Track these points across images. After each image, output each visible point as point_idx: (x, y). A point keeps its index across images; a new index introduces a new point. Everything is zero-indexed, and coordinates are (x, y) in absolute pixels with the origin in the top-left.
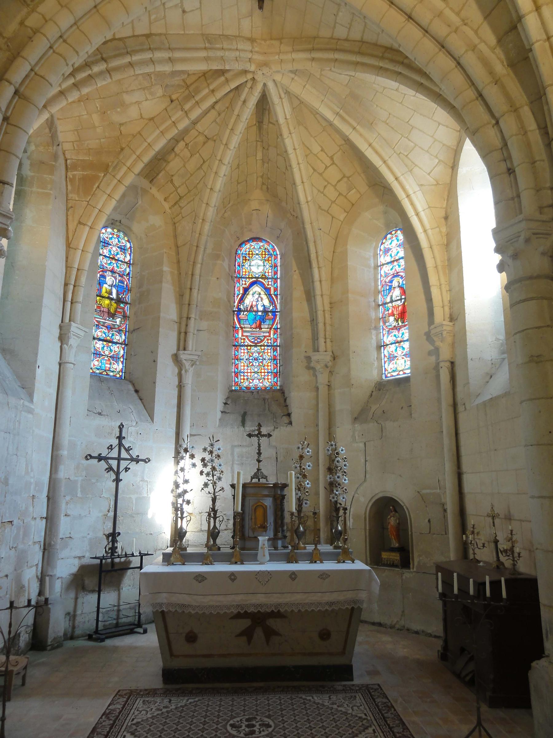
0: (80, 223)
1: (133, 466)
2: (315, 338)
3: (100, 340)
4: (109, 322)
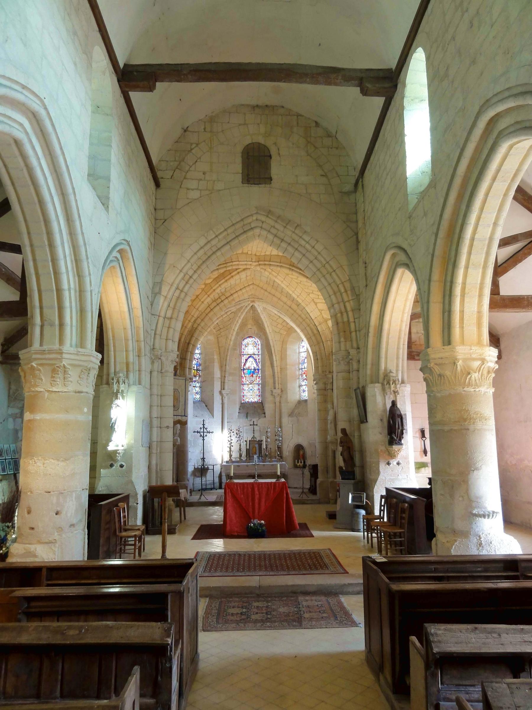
2: (274, 383)
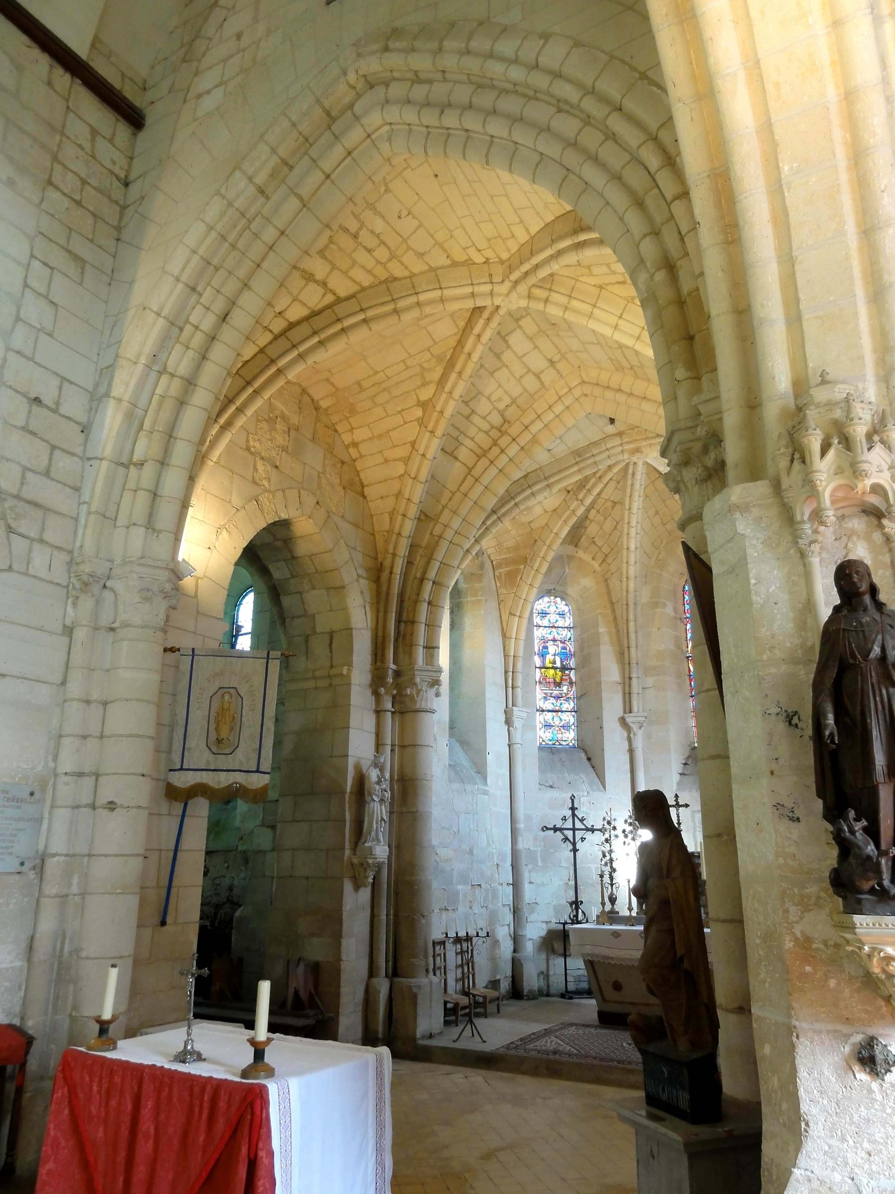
0: (511, 614)
1: (588, 835)
3: (549, 711)
4: (556, 693)
